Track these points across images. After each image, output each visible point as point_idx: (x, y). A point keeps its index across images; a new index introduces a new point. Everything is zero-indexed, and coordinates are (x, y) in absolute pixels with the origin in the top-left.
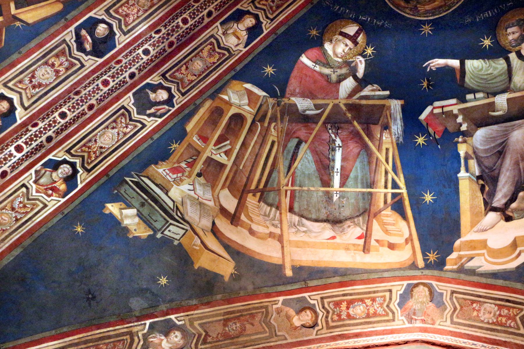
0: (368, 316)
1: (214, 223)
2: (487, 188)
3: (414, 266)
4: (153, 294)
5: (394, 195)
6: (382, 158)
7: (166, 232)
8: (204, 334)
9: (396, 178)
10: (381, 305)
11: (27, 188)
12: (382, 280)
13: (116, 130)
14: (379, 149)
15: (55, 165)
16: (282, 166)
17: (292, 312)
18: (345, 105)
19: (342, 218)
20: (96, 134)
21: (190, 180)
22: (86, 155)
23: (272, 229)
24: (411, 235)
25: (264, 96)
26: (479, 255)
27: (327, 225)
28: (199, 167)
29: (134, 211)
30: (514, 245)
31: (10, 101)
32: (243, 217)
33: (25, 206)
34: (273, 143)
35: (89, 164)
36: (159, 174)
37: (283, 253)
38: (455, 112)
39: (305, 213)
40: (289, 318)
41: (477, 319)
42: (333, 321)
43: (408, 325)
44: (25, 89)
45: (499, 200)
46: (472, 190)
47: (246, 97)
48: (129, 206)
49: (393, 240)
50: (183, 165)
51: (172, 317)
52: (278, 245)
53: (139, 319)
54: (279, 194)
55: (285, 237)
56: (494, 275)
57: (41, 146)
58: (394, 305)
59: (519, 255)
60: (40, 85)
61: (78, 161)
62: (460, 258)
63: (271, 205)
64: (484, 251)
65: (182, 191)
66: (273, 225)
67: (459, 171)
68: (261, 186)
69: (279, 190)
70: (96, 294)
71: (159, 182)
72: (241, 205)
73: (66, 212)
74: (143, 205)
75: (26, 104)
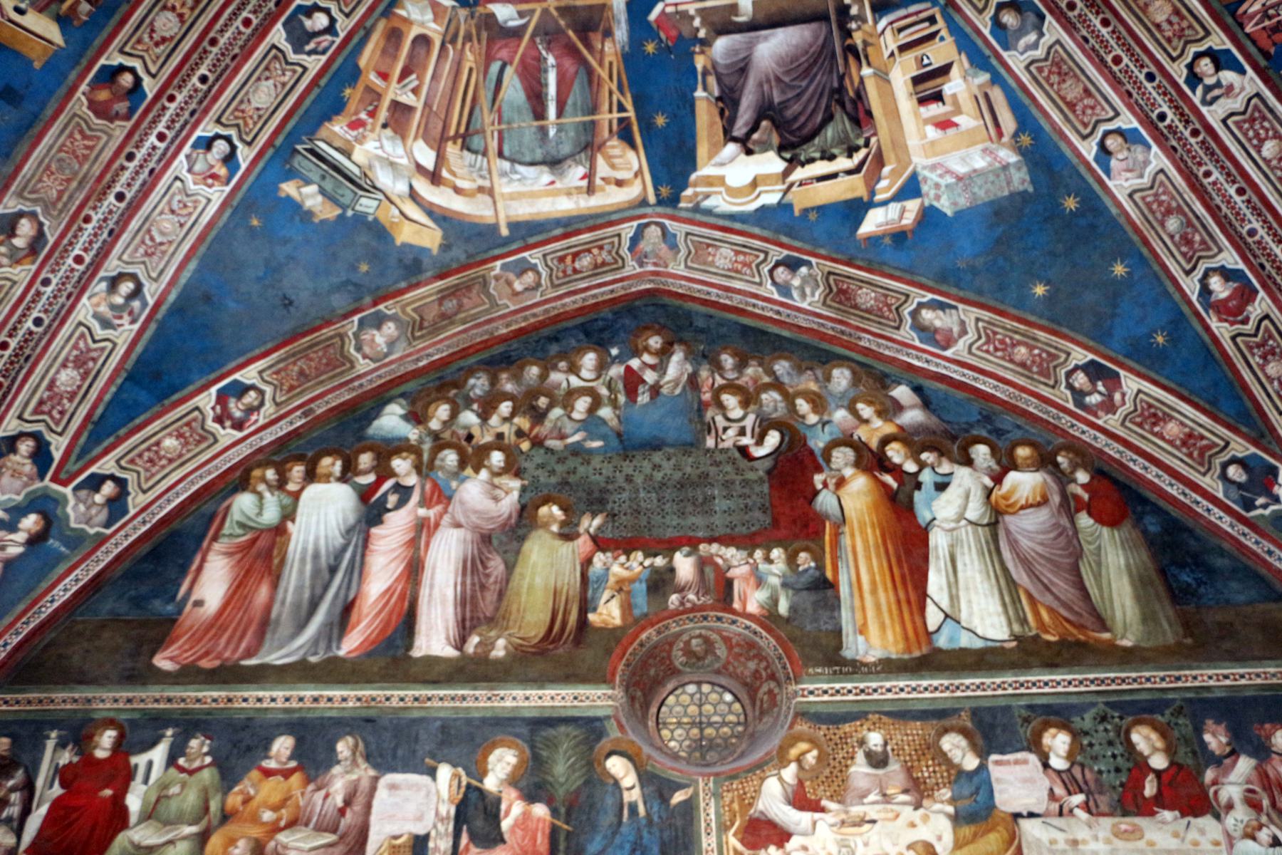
0: (596, 266)
1: (411, 187)
2: (727, 113)
3: (644, 202)
4: (356, 285)
5: (621, 120)
6: (604, 74)
7: (358, 208)
8: (418, 318)
9: (622, 99)
10: (610, 252)
11: (182, 181)
12: (611, 224)
13: (271, 82)
14: (601, 64)
15: (208, 144)
16: (485, 100)
17: (511, 276)
18: (558, 9)
19: (560, 157)
20: (247, 93)
21: (374, 135)
22: (241, 122)
23: (480, 182)
24: (640, 167)
25: (453, 7)
26: (716, 193)
27: (545, 169)
28: (383, 114)
29: (313, 189)
30: (754, 184)
31: (132, 70)
32: (445, 174)
33: (185, 206)
34: (471, 70)
35: (247, 134)
36: (335, 134)
37: (496, 210)
38: (692, 12)
39: (518, 157)
40: (509, 284)
41: (712, 264)
42: (558, 278)
43: (639, 270)
44: (147, 51)
45: (739, 129)
46: (709, 112)
47: (429, 10)
48: (308, 182)
49: (620, 175)
50: (363, 116)
51: (381, 307)
52: (487, 199)
53: (346, 316)
54: (485, 138)
55: (497, 190)
56: (732, 217)
57: (186, 123)
58: (625, 251)
59: (759, 195)
60: (164, 40)
61: (232, 132)
62: (696, 194)
63: (475, 152)
64: (722, 189)
65: (367, 151)
66: (481, 177)
67: (695, 89)
68: (462, 130)
69: (484, 132)
70: (293, 298)
71: (337, 144)
72: (440, 158)
73: (235, 203)
74: (323, 178)
75: (153, 70)
